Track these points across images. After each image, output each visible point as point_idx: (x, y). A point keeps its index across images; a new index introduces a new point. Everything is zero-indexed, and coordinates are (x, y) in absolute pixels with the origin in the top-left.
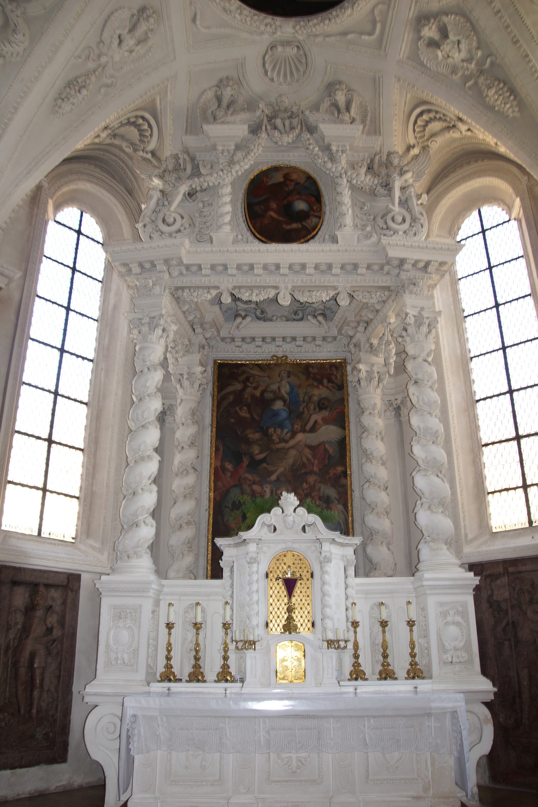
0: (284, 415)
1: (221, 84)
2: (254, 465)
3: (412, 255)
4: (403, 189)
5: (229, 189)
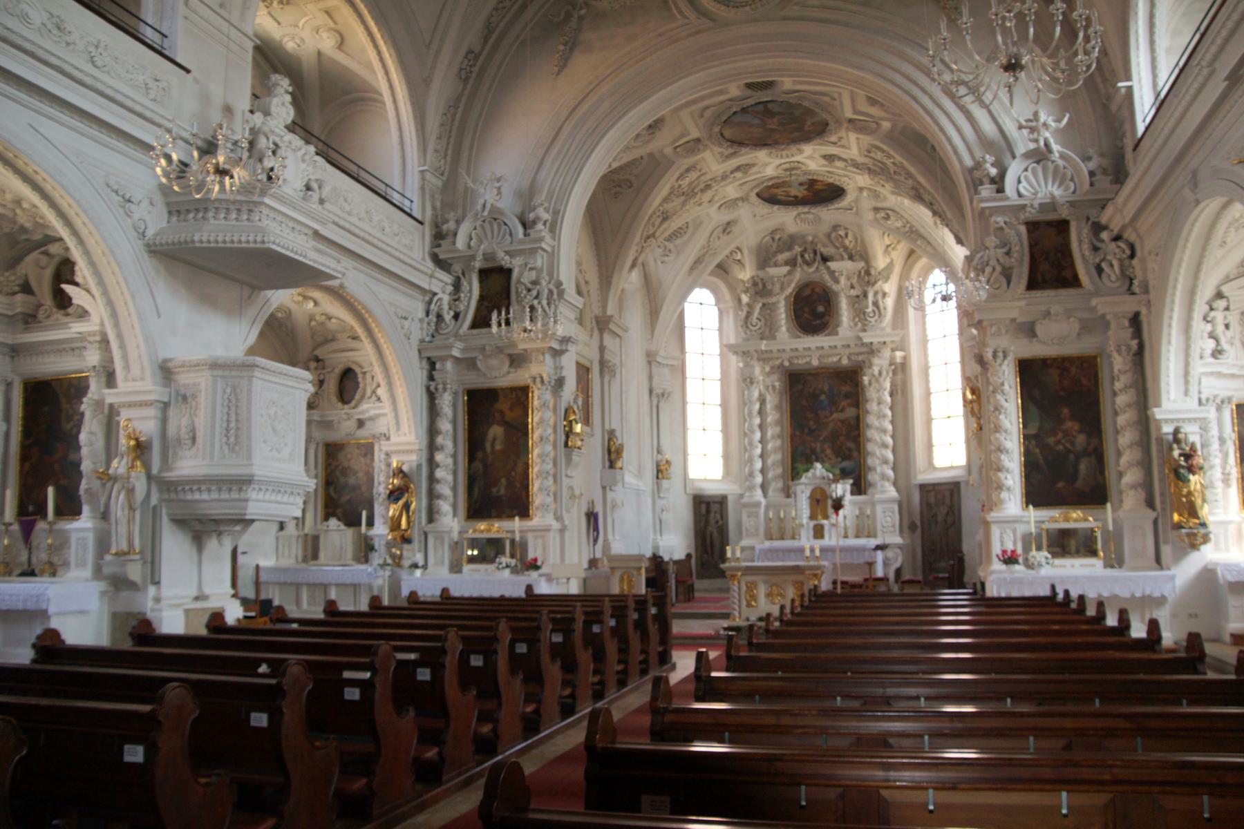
0: (826, 403)
1: (773, 232)
2: (811, 432)
3: (875, 340)
4: (876, 293)
5: (783, 303)
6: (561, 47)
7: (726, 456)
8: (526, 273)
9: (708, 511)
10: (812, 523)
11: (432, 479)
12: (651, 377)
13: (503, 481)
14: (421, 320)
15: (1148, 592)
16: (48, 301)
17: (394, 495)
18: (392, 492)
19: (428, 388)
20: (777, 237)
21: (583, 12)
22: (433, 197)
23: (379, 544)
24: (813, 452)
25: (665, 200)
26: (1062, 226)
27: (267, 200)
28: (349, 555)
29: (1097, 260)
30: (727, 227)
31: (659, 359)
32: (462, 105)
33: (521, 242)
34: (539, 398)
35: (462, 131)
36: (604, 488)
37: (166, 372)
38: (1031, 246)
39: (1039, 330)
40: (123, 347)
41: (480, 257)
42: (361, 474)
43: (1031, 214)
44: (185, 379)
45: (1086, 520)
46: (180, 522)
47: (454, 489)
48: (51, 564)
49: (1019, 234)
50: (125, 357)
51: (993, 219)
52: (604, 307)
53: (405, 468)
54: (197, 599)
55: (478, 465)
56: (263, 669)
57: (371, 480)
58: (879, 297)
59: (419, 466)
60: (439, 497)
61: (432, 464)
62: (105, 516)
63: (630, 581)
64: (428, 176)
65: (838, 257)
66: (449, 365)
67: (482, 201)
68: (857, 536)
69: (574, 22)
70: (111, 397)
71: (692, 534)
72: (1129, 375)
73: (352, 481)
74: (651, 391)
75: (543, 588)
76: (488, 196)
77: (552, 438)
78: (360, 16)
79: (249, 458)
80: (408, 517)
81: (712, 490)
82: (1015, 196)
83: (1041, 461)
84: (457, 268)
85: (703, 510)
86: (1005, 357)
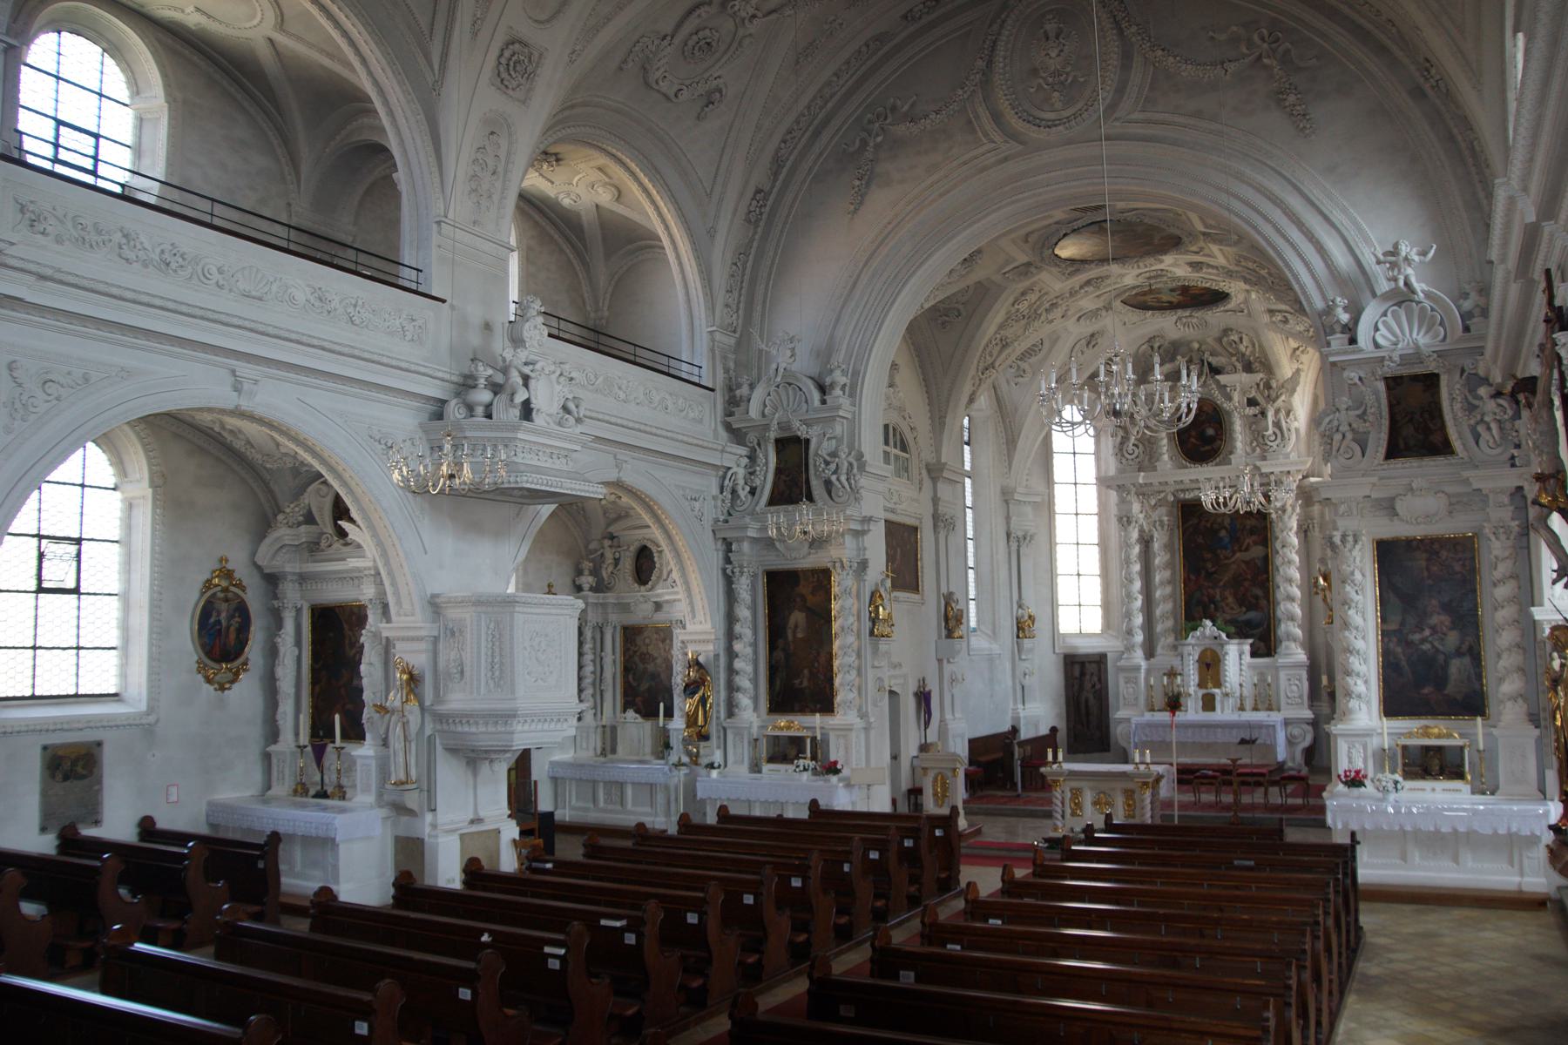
2: (1209, 575)
3: (1277, 470)
4: (1277, 411)
6: (857, 183)
7: (1106, 606)
8: (825, 444)
9: (1083, 674)
10: (1201, 692)
11: (731, 671)
12: (1008, 518)
13: (806, 671)
14: (714, 498)
15: (1514, 829)
16: (329, 529)
17: (691, 689)
18: (687, 686)
19: (724, 570)
20: (1156, 346)
21: (879, 139)
22: (724, 358)
23: (675, 741)
24: (1212, 600)
25: (1001, 327)
26: (1431, 381)
27: (520, 436)
28: (648, 749)
29: (1472, 422)
30: (1092, 340)
31: (1016, 497)
32: (753, 251)
33: (816, 410)
34: (841, 583)
35: (753, 281)
36: (940, 661)
37: (435, 606)
38: (1391, 406)
39: (1399, 506)
40: (394, 584)
41: (774, 425)
42: (659, 661)
43: (1391, 369)
44: (452, 613)
45: (1450, 736)
46: (453, 751)
47: (755, 681)
48: (340, 787)
49: (1376, 393)
50: (397, 593)
51: (1346, 374)
52: (938, 451)
53: (701, 659)
54: (472, 822)
55: (779, 654)
56: (485, 938)
57: (670, 668)
58: (1282, 415)
59: (717, 656)
60: (738, 689)
61: (731, 655)
62: (385, 743)
63: (944, 784)
64: (718, 336)
65: (1229, 368)
66: (746, 546)
67: (774, 366)
68: (1255, 709)
69: (869, 155)
70: (387, 630)
71: (1063, 700)
72: (1509, 563)
73: (651, 667)
74: (1008, 535)
75: (842, 799)
76: (782, 359)
77: (855, 628)
78: (633, 174)
79: (513, 692)
80: (705, 712)
81: (1085, 647)
82: (1371, 347)
83: (1404, 663)
84: (752, 437)
85: (1077, 673)
86: (1356, 542)
